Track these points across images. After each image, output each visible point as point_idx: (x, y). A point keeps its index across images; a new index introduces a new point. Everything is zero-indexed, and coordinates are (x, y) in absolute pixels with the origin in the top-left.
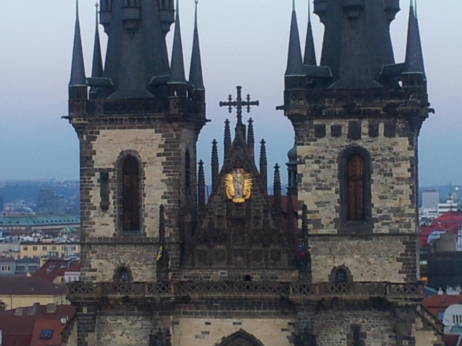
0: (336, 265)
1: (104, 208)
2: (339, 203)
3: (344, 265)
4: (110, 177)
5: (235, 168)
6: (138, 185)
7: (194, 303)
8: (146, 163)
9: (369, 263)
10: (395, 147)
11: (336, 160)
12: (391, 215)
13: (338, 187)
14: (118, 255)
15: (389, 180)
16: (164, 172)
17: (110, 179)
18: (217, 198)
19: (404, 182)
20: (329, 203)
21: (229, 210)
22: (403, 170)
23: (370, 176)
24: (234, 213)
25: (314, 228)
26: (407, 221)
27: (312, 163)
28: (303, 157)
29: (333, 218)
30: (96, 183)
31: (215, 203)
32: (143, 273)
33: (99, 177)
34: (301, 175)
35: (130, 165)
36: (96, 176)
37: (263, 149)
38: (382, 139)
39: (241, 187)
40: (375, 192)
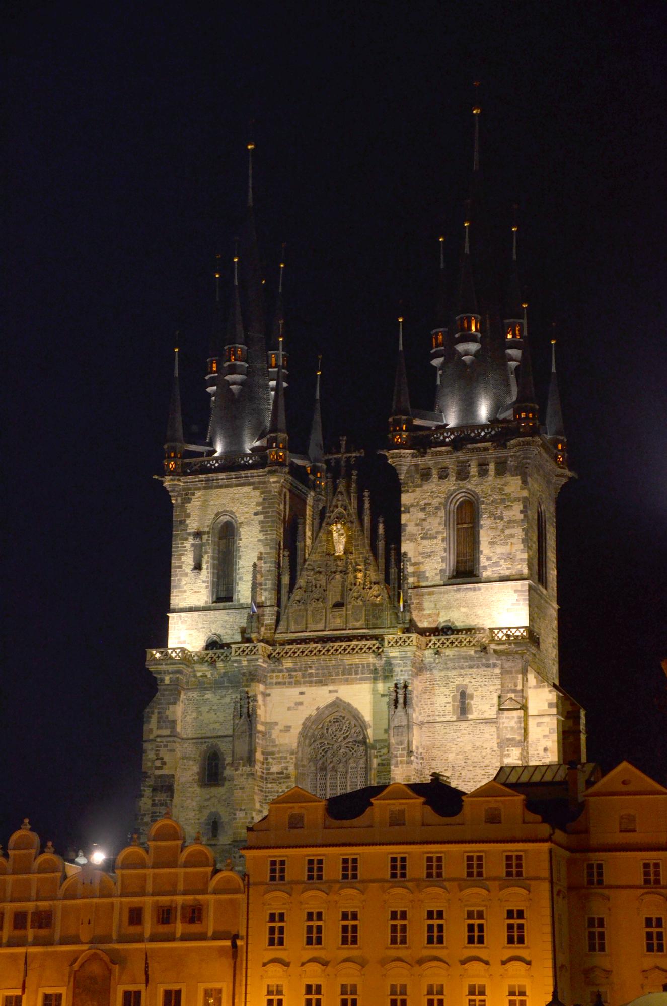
2: (445, 551)
7: (288, 670)
8: (242, 523)
12: (502, 562)
15: (501, 524)
16: (261, 531)
22: (515, 513)
23: (479, 521)
40: (484, 537)
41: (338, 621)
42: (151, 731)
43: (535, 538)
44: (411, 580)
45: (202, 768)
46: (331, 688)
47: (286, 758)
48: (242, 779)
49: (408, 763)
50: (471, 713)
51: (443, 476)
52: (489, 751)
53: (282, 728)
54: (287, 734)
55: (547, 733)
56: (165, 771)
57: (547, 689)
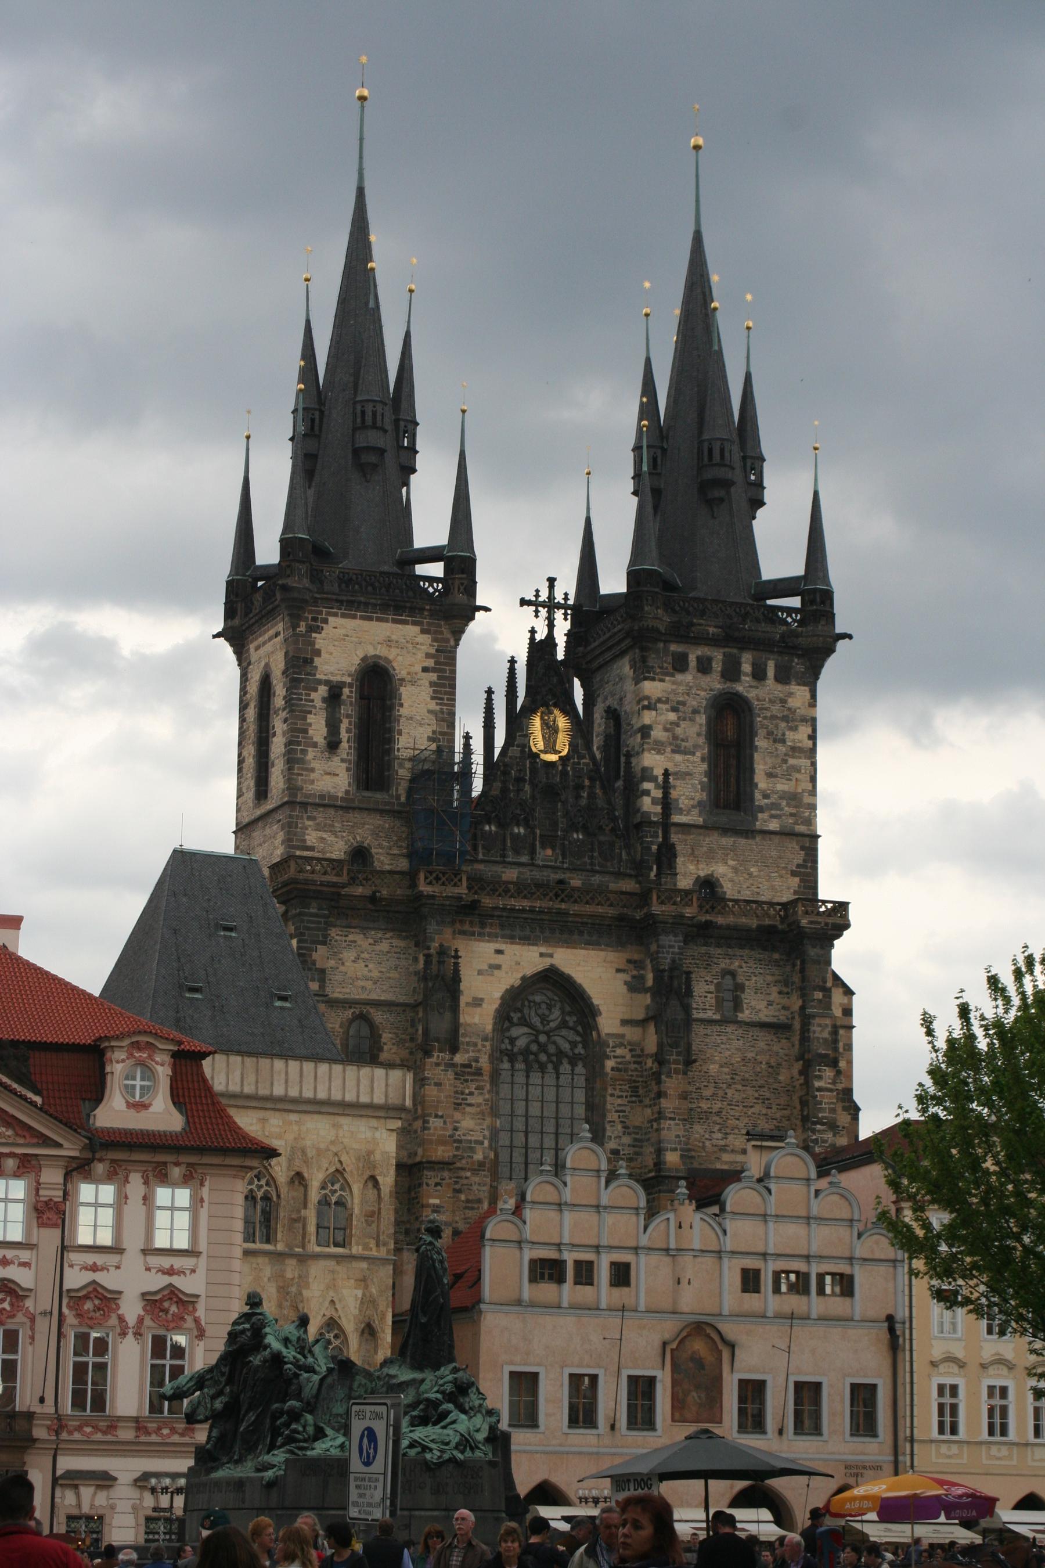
0: (702, 874)
3: (712, 875)
4: (344, 697)
5: (547, 706)
6: (390, 716)
7: (479, 915)
8: (403, 680)
9: (750, 875)
10: (790, 700)
11: (702, 711)
12: (784, 803)
13: (706, 751)
14: (352, 827)
15: (782, 749)
16: (433, 698)
17: (344, 701)
18: (514, 751)
19: (802, 755)
20: (690, 774)
21: (534, 770)
23: (752, 741)
26: (807, 814)
27: (667, 710)
28: (654, 698)
29: (697, 798)
30: (319, 704)
31: (511, 757)
33: (326, 695)
34: (649, 728)
36: (320, 692)
38: (771, 686)
40: (760, 767)
41: (549, 852)
46: (543, 950)
47: (475, 1045)
49: (685, 1073)
50: (742, 1011)
51: (704, 666)
53: (470, 1000)
54: (478, 1010)
57: (841, 990)
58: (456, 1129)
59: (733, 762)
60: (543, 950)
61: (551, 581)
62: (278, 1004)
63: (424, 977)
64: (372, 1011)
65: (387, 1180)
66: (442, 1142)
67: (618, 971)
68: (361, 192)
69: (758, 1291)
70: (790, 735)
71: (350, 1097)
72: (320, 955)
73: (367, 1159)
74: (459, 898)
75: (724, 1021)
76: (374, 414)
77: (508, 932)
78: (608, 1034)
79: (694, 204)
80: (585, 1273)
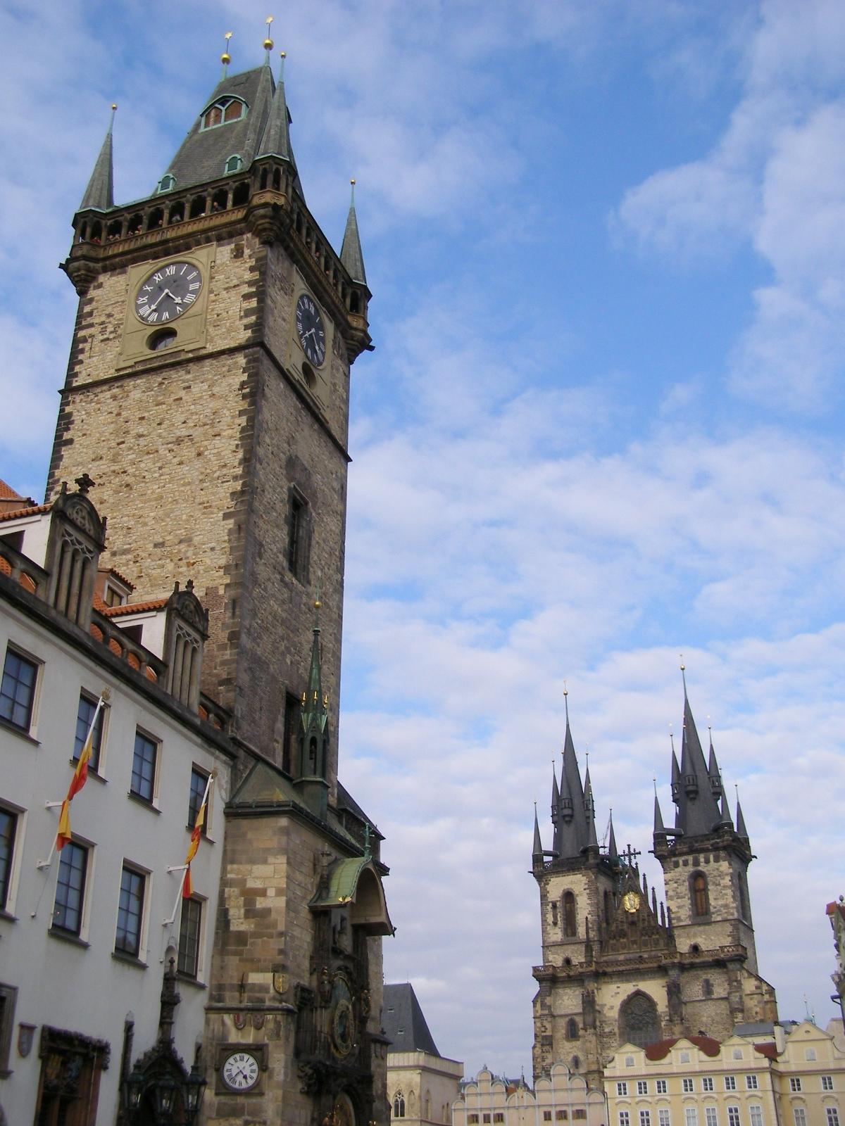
0: (692, 943)
1: (555, 924)
5: (629, 892)
9: (711, 940)
12: (722, 909)
13: (689, 895)
18: (620, 912)
21: (627, 918)
22: (727, 881)
24: (630, 919)
25: (677, 922)
32: (578, 957)
35: (569, 896)
37: (645, 879)
39: (633, 902)
40: (711, 896)
41: (635, 946)
42: (537, 1011)
43: (739, 895)
44: (673, 921)
45: (567, 1031)
46: (634, 984)
48: (590, 1036)
52: (725, 1015)
54: (612, 1011)
55: (756, 1003)
56: (548, 1033)
57: (754, 979)
58: (608, 1057)
59: (704, 897)
60: (634, 984)
61: (629, 846)
62: (399, 1033)
63: (583, 1003)
64: (575, 1017)
65: (417, 1092)
66: (593, 1063)
67: (663, 987)
68: (568, 726)
69: (550, 1119)
70: (722, 882)
71: (401, 1064)
72: (548, 1000)
73: (409, 1085)
74: (592, 971)
75: (708, 1000)
76: (565, 803)
77: (620, 979)
78: (661, 1012)
79: (683, 690)
80: (487, 1119)
